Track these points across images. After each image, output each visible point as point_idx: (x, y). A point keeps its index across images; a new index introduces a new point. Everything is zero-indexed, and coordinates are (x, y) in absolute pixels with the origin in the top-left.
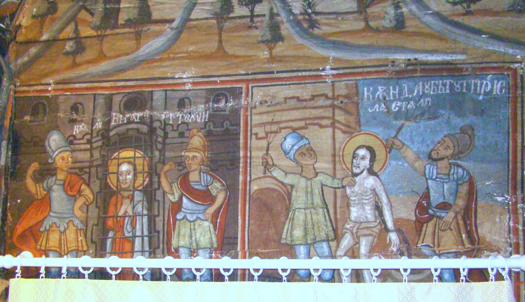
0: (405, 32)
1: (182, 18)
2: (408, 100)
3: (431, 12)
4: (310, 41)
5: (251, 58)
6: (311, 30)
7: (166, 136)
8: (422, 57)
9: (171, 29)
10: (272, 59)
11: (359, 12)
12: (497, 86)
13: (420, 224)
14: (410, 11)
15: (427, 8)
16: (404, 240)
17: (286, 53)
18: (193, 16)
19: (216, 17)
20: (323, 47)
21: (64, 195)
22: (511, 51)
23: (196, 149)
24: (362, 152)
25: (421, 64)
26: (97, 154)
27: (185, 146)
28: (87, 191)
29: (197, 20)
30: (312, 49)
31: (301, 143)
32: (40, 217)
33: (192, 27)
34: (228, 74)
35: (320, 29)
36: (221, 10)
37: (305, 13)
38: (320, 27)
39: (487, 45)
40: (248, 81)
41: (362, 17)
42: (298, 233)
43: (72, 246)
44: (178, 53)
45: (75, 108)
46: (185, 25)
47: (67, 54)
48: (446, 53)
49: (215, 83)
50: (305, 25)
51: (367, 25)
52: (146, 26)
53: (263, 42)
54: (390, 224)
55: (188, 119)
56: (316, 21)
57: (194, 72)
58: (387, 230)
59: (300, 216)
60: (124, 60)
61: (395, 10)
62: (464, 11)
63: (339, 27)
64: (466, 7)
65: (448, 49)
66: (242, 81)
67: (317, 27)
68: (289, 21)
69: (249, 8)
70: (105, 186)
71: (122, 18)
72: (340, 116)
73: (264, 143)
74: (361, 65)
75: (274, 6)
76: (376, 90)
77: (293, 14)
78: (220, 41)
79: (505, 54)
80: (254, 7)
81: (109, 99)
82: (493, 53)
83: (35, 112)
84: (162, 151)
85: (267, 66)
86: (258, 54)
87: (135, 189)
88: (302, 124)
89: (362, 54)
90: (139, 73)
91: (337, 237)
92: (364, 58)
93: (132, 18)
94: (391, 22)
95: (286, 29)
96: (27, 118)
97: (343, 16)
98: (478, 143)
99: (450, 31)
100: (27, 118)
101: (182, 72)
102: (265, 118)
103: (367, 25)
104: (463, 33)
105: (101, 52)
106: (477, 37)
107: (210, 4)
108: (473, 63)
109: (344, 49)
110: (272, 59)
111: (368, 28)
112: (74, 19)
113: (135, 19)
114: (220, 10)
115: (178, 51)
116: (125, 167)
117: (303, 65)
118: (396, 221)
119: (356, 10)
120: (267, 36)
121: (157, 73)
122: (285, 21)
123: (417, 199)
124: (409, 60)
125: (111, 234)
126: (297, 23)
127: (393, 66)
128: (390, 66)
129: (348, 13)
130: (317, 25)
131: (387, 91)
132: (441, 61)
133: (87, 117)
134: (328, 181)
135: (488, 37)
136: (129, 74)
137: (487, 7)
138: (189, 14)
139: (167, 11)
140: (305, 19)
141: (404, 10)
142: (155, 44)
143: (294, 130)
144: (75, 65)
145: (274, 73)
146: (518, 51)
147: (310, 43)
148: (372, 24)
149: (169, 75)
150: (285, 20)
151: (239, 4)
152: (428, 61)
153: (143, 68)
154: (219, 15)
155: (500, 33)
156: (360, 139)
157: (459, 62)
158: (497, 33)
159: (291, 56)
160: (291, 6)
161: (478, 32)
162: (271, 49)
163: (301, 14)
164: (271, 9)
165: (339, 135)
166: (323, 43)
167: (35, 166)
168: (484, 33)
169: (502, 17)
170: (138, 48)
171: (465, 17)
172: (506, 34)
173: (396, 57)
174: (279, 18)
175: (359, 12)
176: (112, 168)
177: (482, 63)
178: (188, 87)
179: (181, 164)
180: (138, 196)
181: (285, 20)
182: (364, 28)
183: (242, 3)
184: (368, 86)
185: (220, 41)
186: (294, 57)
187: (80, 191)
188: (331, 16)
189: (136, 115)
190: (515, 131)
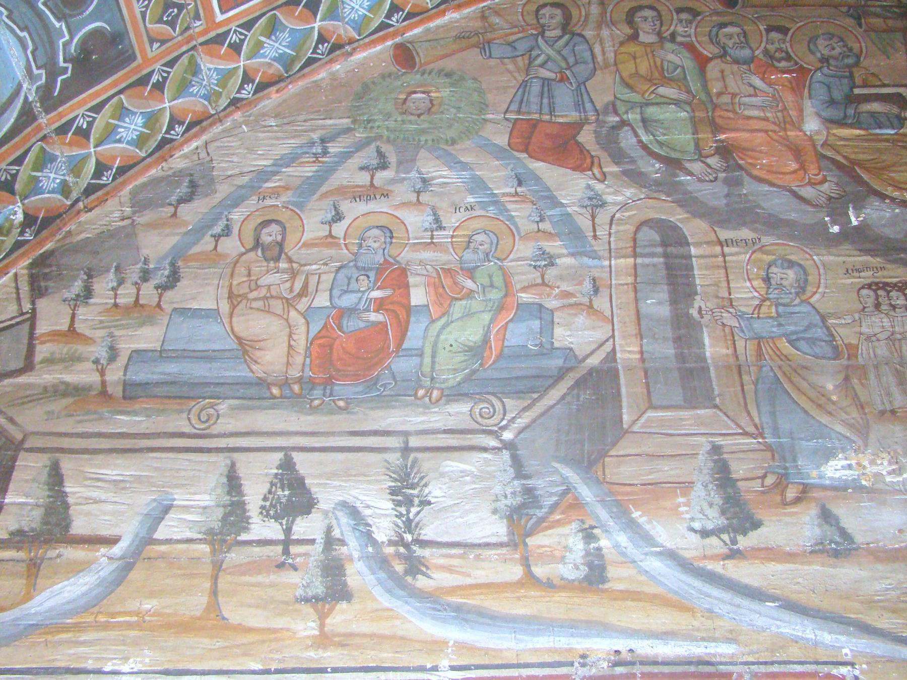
0: (606, 590)
1: (136, 535)
3: (658, 549)
4: (406, 602)
5: (278, 635)
6: (409, 579)
8: (646, 648)
9: (110, 558)
10: (324, 639)
11: (512, 544)
14: (617, 546)
15: (649, 540)
17: (355, 628)
18: (159, 535)
19: (209, 538)
20: (434, 618)
22: (827, 638)
25: (642, 663)
29: (168, 541)
30: (411, 622)
33: (156, 559)
34: (225, 668)
35: (429, 577)
36: (223, 526)
37: (401, 542)
38: (428, 572)
39: (778, 623)
41: (517, 556)
44: (120, 613)
46: (140, 553)
48: (689, 636)
50: (399, 568)
51: (529, 574)
52: (56, 549)
53: (307, 600)
56: (421, 561)
57: (147, 660)
61: (585, 543)
62: (725, 550)
63: (469, 576)
64: (728, 541)
65: (698, 630)
67: (424, 574)
68: (366, 558)
69: (281, 524)
74: (515, 662)
75: (334, 522)
77: (374, 543)
78: (214, 592)
79: (816, 644)
80: (293, 522)
82: (793, 640)
85: (313, 656)
86: (293, 626)
89: (518, 636)
92: (522, 646)
93: (26, 529)
94: (577, 567)
97: (480, 551)
99: (700, 591)
101: (121, 659)
103: (529, 574)
104: (727, 596)
106: (755, 605)
107: (201, 510)
108: (753, 663)
109: (477, 622)
113: (33, 530)
114: (220, 524)
115: (118, 608)
117: (390, 655)
119: (505, 539)
120: (316, 588)
122: (357, 556)
124: (617, 652)
126: (384, 563)
127: (583, 665)
128: (576, 664)
129: (487, 545)
130: (424, 569)
132: (684, 657)
135: (780, 606)
137: (771, 544)
138: (153, 528)
139: (106, 518)
140: (398, 555)
141: (604, 543)
142: (69, 588)
145: (327, 672)
146: (843, 638)
147: (407, 607)
148: (539, 571)
149: (90, 664)
150: (356, 555)
151: (261, 513)
152: (657, 655)
153: (35, 644)
154: (216, 535)
155: (803, 599)
157: (723, 660)
158: (794, 597)
159: (365, 635)
160: (370, 526)
161: (756, 594)
162: (322, 617)
163: (391, 543)
164: (329, 530)
166: (434, 609)
168: (774, 599)
169: (802, 563)
170: (28, 597)
171: (726, 562)
172: (815, 601)
173: (588, 646)
174: (344, 549)
175: (512, 544)
177: (772, 663)
181: (356, 555)
182: (522, 578)
183: (268, 512)
185: (214, 592)
186: (372, 636)
188: (454, 551)
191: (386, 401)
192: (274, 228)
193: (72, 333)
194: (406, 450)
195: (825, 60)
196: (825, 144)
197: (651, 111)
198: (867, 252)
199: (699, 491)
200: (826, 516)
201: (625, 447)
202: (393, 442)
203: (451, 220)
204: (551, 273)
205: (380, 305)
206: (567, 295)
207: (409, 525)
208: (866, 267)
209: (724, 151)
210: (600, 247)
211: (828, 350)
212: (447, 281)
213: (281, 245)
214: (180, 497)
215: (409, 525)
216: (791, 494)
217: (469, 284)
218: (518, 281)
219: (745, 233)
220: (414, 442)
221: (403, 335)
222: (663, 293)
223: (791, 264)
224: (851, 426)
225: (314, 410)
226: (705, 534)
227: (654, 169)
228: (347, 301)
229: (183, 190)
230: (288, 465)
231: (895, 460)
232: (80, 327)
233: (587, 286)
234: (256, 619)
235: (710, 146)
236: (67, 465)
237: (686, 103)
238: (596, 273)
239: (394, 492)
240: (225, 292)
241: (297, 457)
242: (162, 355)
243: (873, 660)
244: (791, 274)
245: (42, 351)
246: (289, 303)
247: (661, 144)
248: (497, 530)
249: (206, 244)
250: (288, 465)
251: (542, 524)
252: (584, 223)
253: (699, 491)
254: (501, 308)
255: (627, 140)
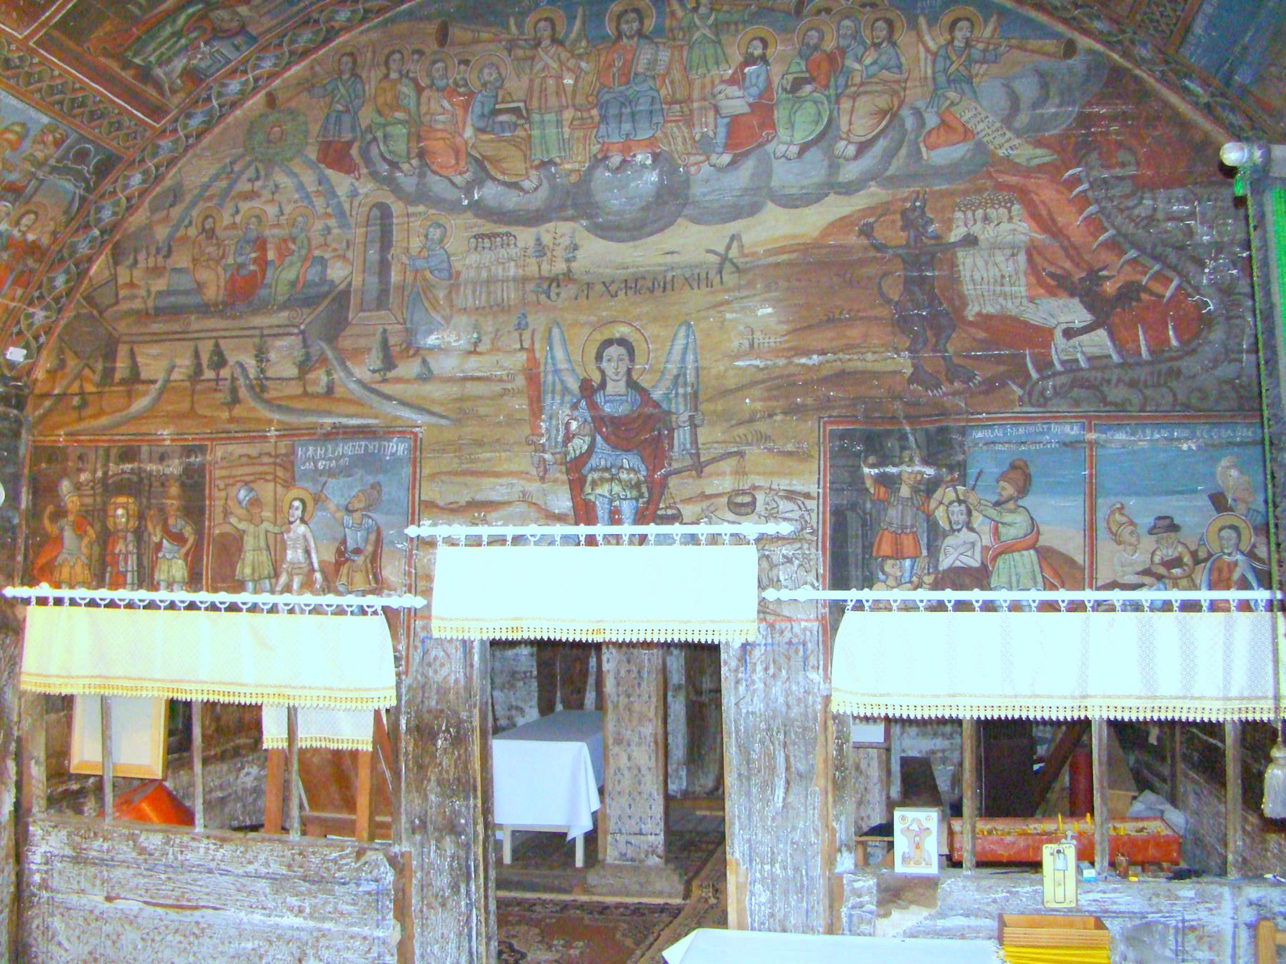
2: (330, 459)
7: (151, 486)
8: (345, 421)
10: (232, 420)
12: (401, 447)
13: (338, 565)
16: (325, 578)
18: (172, 378)
21: (73, 535)
22: (414, 416)
23: (173, 498)
24: (297, 503)
26: (99, 499)
27: (165, 495)
28: (91, 531)
31: (251, 495)
32: (54, 554)
40: (212, 440)
42: (248, 571)
43: (80, 578)
45: (81, 458)
47: (74, 408)
49: (186, 440)
50: (258, 390)
54: (316, 566)
55: (168, 471)
58: (313, 570)
59: (249, 556)
60: (118, 417)
66: (208, 439)
70: (105, 527)
71: (118, 376)
72: (280, 473)
73: (223, 494)
76: (307, 450)
81: (108, 450)
83: (49, 461)
84: (149, 498)
87: (127, 531)
88: (252, 478)
90: (133, 429)
91: (277, 575)
95: (243, 393)
96: (44, 465)
98: (385, 497)
100: (44, 465)
102: (224, 473)
105: (101, 409)
110: (232, 420)
111: (305, 394)
112: (79, 376)
116: (120, 512)
118: (321, 562)
121: (144, 429)
123: (337, 544)
125: (109, 569)
131: (315, 451)
133: (90, 466)
134: (271, 528)
136: (123, 429)
141: (335, 376)
143: (246, 483)
144: (80, 419)
148: (310, 389)
156: (294, 493)
161: (389, 398)
162: (230, 411)
165: (280, 489)
167: (50, 509)
170: (129, 406)
176: (111, 513)
178: (168, 443)
179: (162, 510)
180: (130, 537)
184: (302, 446)
185: (193, 402)
187: (85, 532)
189: (128, 467)
190: (414, 487)
191: (255, 312)
192: (210, 220)
193: (131, 285)
194: (262, 336)
195: (484, 85)
196: (473, 146)
197: (389, 129)
198: (477, 216)
199: (374, 352)
200: (424, 362)
201: (348, 331)
202: (257, 332)
203: (288, 209)
204: (329, 238)
205: (255, 261)
206: (335, 250)
207: (262, 371)
208: (475, 225)
209: (422, 154)
210: (352, 221)
211: (445, 274)
212: (283, 246)
213: (213, 230)
214: (178, 362)
215: (262, 371)
216: (411, 352)
217: (293, 247)
218: (314, 243)
219: (421, 208)
220: (266, 332)
221: (263, 277)
222: (377, 246)
223: (440, 226)
224: (443, 317)
225: (228, 318)
226: (374, 371)
227: (384, 168)
228: (240, 260)
229: (171, 198)
230: (217, 345)
231: (458, 335)
232: (136, 281)
233: (344, 244)
234: (207, 412)
235: (414, 152)
236: (136, 348)
237: (407, 122)
238: (349, 237)
239: (256, 356)
240: (190, 258)
241: (222, 342)
242: (168, 293)
243: (429, 425)
244: (438, 231)
245: (122, 293)
246: (218, 262)
247: (390, 152)
248: (293, 371)
249: (181, 233)
250: (217, 345)
251: (312, 369)
252: (347, 207)
253: (374, 352)
254: (306, 259)
255: (374, 152)
